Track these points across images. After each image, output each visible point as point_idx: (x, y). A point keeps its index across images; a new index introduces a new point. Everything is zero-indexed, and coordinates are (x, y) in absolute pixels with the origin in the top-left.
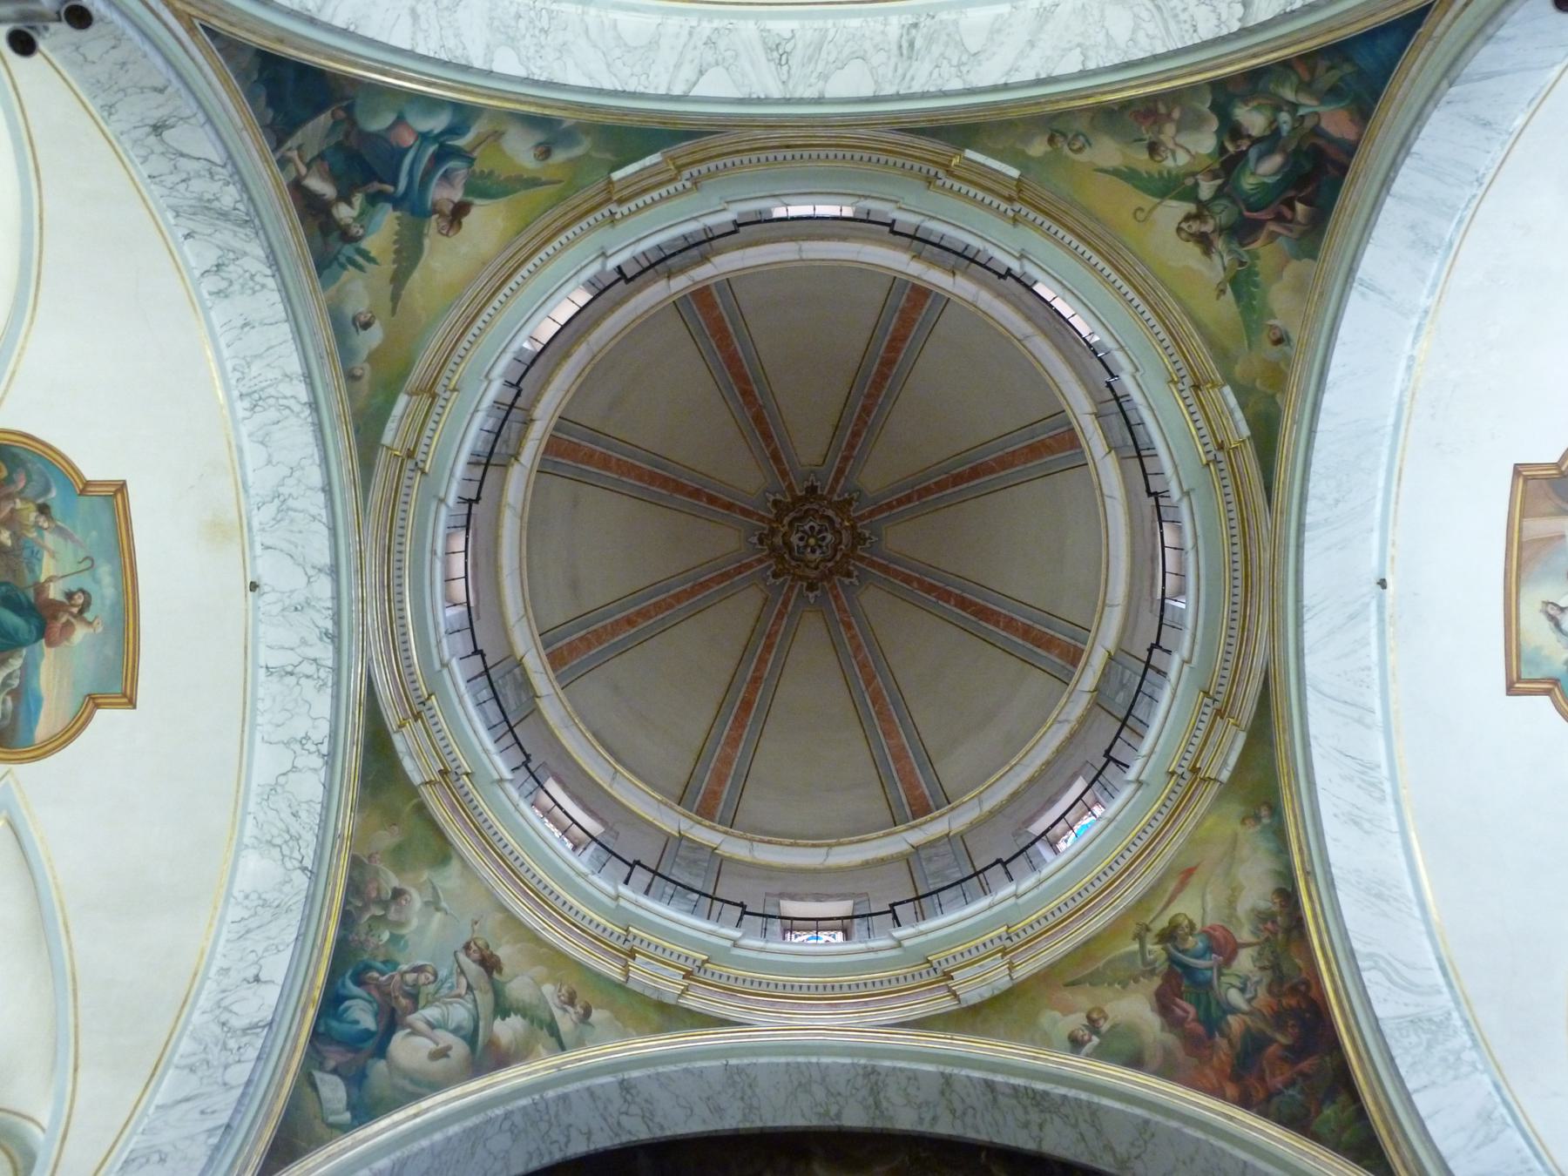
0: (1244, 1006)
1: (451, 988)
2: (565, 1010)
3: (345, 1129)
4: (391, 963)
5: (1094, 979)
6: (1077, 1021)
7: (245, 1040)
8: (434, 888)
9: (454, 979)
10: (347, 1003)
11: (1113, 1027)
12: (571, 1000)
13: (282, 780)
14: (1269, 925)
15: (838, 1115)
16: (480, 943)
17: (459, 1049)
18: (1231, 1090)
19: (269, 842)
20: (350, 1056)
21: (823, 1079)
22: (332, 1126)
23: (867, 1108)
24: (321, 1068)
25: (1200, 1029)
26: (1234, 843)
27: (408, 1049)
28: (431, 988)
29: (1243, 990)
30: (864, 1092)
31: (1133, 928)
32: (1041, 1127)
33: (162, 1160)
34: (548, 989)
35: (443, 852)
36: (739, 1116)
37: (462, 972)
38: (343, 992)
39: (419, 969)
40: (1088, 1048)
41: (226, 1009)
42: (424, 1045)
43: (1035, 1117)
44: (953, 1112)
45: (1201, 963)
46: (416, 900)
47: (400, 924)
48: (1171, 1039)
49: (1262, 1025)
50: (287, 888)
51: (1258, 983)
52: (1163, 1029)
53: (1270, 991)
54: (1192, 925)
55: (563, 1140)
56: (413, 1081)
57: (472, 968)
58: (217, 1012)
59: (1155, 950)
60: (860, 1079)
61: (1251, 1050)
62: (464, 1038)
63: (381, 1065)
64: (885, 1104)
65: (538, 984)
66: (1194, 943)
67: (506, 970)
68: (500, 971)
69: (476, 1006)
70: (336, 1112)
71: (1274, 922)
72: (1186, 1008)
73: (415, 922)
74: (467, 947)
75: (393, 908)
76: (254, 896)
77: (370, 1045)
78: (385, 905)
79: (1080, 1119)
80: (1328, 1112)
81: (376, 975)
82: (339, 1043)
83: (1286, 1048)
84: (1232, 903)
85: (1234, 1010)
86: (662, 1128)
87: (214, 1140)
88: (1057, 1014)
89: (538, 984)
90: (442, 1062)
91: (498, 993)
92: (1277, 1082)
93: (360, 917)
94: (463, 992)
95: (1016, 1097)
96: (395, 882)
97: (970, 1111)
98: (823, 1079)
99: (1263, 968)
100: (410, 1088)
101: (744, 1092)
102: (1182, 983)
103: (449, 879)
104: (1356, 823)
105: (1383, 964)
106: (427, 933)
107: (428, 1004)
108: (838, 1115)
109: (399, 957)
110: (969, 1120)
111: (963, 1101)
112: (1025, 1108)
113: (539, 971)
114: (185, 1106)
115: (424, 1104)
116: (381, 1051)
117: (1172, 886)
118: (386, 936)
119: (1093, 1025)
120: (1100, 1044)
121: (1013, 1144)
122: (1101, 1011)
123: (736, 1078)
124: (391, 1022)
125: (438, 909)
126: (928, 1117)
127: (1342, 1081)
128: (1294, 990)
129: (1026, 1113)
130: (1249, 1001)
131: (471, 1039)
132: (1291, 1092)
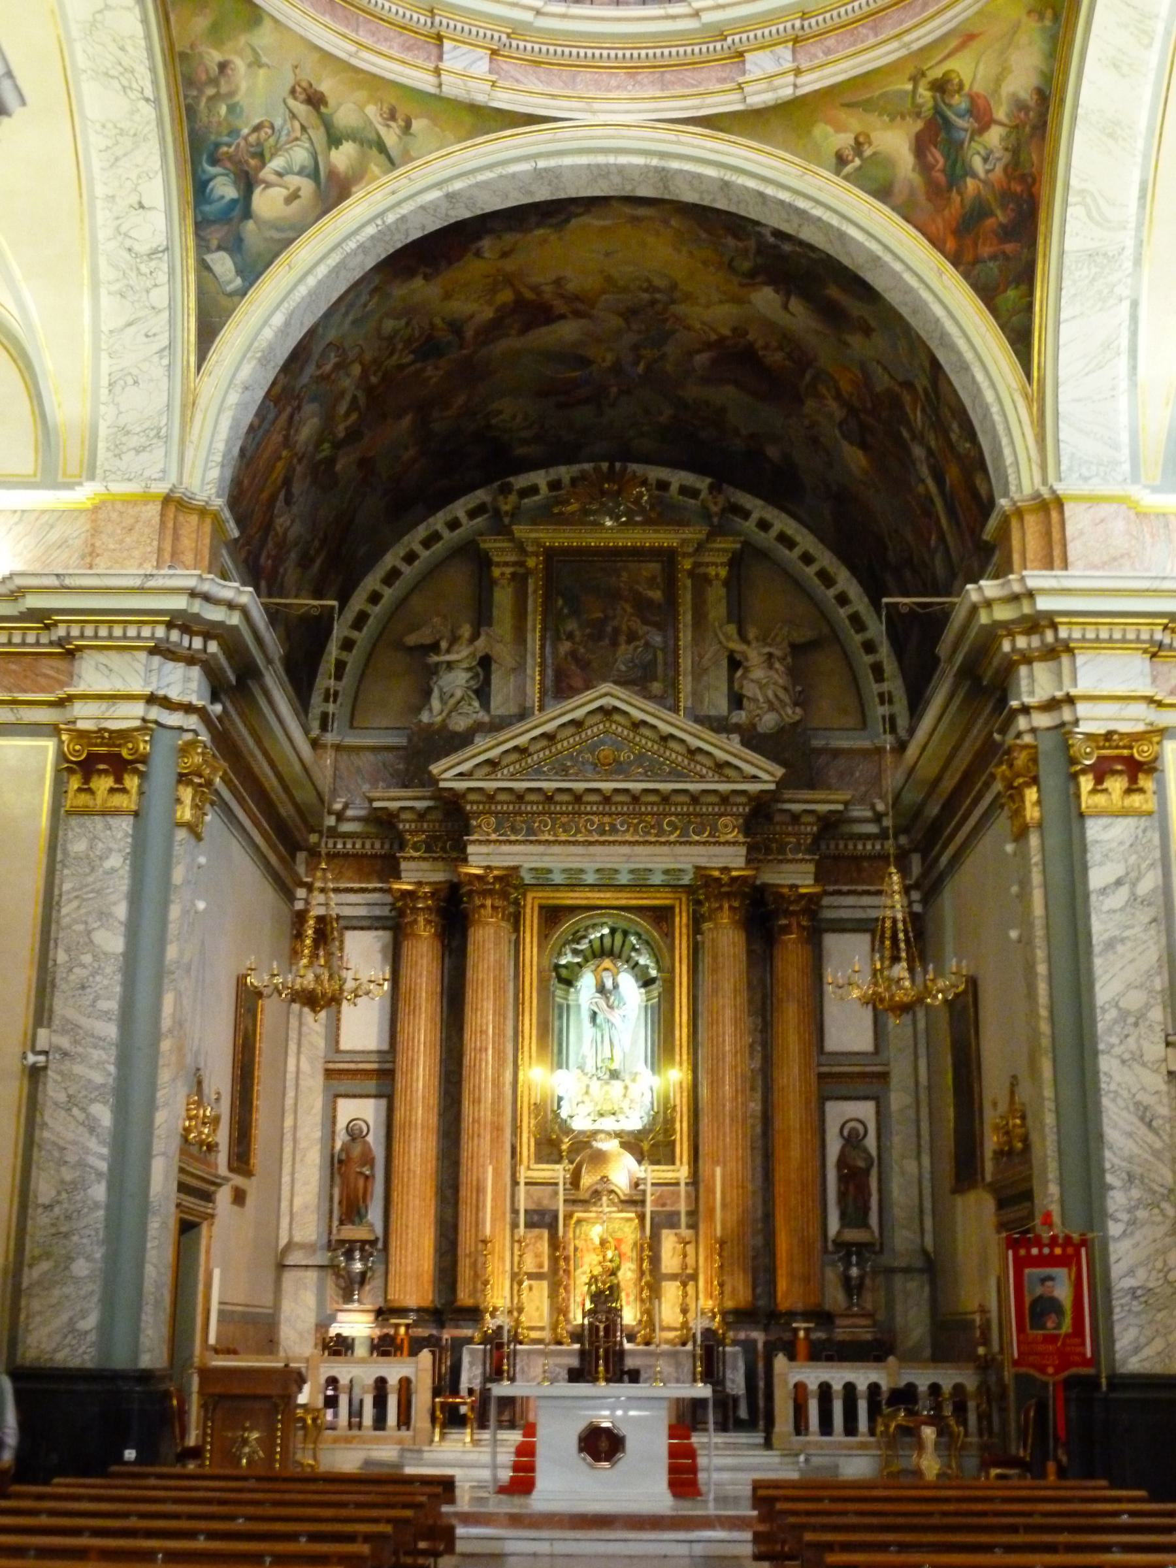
0: (982, 174)
1: (288, 134)
2: (388, 126)
3: (243, 293)
4: (234, 132)
5: (867, 106)
6: (844, 140)
7: (153, 264)
8: (253, 50)
9: (289, 125)
10: (211, 184)
11: (875, 154)
12: (392, 116)
13: (99, 17)
14: (1022, 115)
16: (304, 84)
17: (306, 186)
18: (951, 244)
19: (106, 74)
20: (226, 228)
22: (230, 295)
24: (209, 250)
25: (941, 178)
26: (1016, 28)
27: (268, 202)
28: (272, 141)
29: (985, 160)
31: (910, 70)
33: (136, 382)
37: (294, 116)
38: (205, 177)
39: (257, 128)
40: (849, 169)
41: (126, 235)
42: (277, 194)
45: (960, 123)
46: (240, 64)
47: (232, 94)
48: (916, 179)
49: (990, 197)
50: (137, 117)
51: (999, 159)
52: (914, 170)
53: (1005, 169)
54: (961, 86)
56: (279, 229)
57: (301, 109)
58: (120, 238)
59: (925, 95)
61: (975, 215)
62: (308, 176)
63: (250, 225)
64: (672, 188)
65: (361, 108)
66: (960, 102)
67: (331, 101)
68: (326, 104)
69: (312, 143)
70: (230, 282)
71: (1027, 114)
72: (937, 157)
73: (244, 86)
74: (293, 92)
75: (223, 82)
76: (109, 125)
77: (237, 213)
78: (214, 82)
81: (225, 149)
82: (214, 222)
83: (1001, 225)
84: (998, 81)
85: (974, 175)
87: (165, 362)
88: (830, 129)
89: (361, 108)
90: (296, 204)
91: (327, 125)
92: (985, 251)
93: (198, 104)
94: (298, 134)
96: (215, 56)
99: (1006, 149)
100: (277, 235)
102: (938, 135)
103: (264, 37)
104: (1116, 66)
105: (1088, 200)
106: (257, 93)
107: (273, 155)
108: (633, 190)
109: (238, 123)
113: (361, 95)
114: (133, 329)
116: (247, 214)
117: (953, 43)
118: (223, 110)
119: (858, 147)
120: (860, 168)
122: (868, 136)
124: (248, 183)
125: (260, 65)
127: (1025, 275)
128: (1022, 178)
130: (988, 172)
131: (315, 175)
132: (991, 264)
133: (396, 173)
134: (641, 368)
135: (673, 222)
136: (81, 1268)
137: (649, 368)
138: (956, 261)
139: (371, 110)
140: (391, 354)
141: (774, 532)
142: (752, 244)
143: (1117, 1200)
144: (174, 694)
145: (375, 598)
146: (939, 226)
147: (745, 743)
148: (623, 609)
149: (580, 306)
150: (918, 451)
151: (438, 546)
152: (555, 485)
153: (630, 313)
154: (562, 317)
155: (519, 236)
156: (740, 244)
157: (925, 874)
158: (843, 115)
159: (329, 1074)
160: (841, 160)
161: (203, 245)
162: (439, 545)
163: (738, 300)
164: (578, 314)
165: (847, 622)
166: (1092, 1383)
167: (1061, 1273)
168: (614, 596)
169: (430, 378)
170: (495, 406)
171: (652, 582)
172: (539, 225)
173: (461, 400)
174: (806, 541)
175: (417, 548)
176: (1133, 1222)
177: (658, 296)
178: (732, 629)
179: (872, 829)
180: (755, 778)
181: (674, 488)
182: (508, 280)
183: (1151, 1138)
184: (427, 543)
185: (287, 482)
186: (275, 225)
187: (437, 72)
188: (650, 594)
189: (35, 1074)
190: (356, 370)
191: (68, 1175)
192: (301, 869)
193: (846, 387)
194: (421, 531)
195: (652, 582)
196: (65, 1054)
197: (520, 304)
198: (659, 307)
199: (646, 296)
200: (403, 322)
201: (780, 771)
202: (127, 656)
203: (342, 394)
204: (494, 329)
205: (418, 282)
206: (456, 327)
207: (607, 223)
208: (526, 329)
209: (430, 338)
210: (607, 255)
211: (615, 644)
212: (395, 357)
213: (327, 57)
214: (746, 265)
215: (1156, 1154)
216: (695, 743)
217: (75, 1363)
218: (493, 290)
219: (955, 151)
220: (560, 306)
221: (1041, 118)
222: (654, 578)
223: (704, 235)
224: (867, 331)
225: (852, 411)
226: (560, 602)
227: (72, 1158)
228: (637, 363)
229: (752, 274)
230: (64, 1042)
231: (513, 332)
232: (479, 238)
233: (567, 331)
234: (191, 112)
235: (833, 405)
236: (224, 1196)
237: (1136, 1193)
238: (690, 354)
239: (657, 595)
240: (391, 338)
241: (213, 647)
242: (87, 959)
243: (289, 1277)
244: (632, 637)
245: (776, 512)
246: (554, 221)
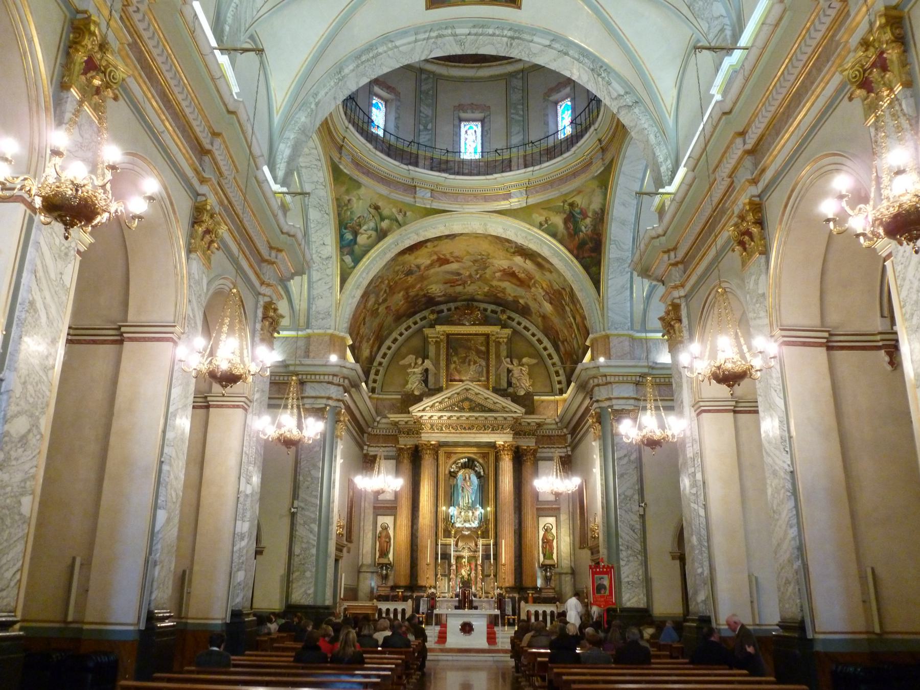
3: (354, 267)
4: (352, 219)
5: (549, 209)
6: (542, 219)
12: (401, 211)
17: (374, 234)
18: (575, 252)
27: (362, 239)
34: (394, 210)
35: (358, 185)
46: (354, 200)
48: (565, 232)
57: (372, 211)
59: (567, 207)
63: (356, 247)
66: (577, 210)
72: (571, 225)
73: (355, 206)
78: (346, 205)
84: (589, 205)
92: (586, 255)
96: (347, 198)
102: (571, 218)
103: (362, 191)
106: (359, 207)
115: (370, 254)
119: (546, 221)
124: (356, 234)
127: (598, 264)
131: (376, 230)
133: (403, 228)
136: (308, 574)
138: (577, 257)
139: (394, 210)
141: (522, 326)
143: (623, 554)
144: (334, 396)
146: (571, 246)
147: (513, 401)
149: (458, 259)
150: (567, 309)
152: (449, 310)
153: (475, 261)
157: (572, 442)
158: (542, 211)
159: (375, 508)
160: (541, 225)
161: (342, 254)
164: (458, 261)
166: (615, 610)
167: (606, 576)
168: (470, 349)
173: (419, 286)
174: (533, 329)
175: (403, 331)
176: (628, 561)
178: (508, 360)
179: (554, 427)
181: (489, 310)
182: (436, 253)
183: (634, 535)
184: (406, 330)
185: (364, 319)
186: (363, 246)
187: (414, 198)
189: (293, 515)
190: (386, 282)
191: (304, 546)
192: (366, 439)
193: (545, 286)
194: (405, 325)
196: (303, 508)
197: (439, 259)
201: (524, 410)
202: (320, 384)
204: (431, 265)
206: (418, 267)
208: (440, 266)
211: (469, 365)
213: (381, 196)
214: (512, 250)
215: (636, 540)
216: (496, 400)
217: (306, 603)
219: (576, 223)
220: (452, 259)
221: (601, 217)
224: (551, 272)
225: (547, 293)
227: (305, 541)
229: (514, 253)
230: (302, 505)
234: (339, 215)
235: (541, 291)
236: (345, 550)
237: (629, 552)
238: (494, 273)
239: (483, 348)
240: (397, 272)
241: (346, 381)
242: (309, 479)
243: (362, 575)
244: (475, 363)
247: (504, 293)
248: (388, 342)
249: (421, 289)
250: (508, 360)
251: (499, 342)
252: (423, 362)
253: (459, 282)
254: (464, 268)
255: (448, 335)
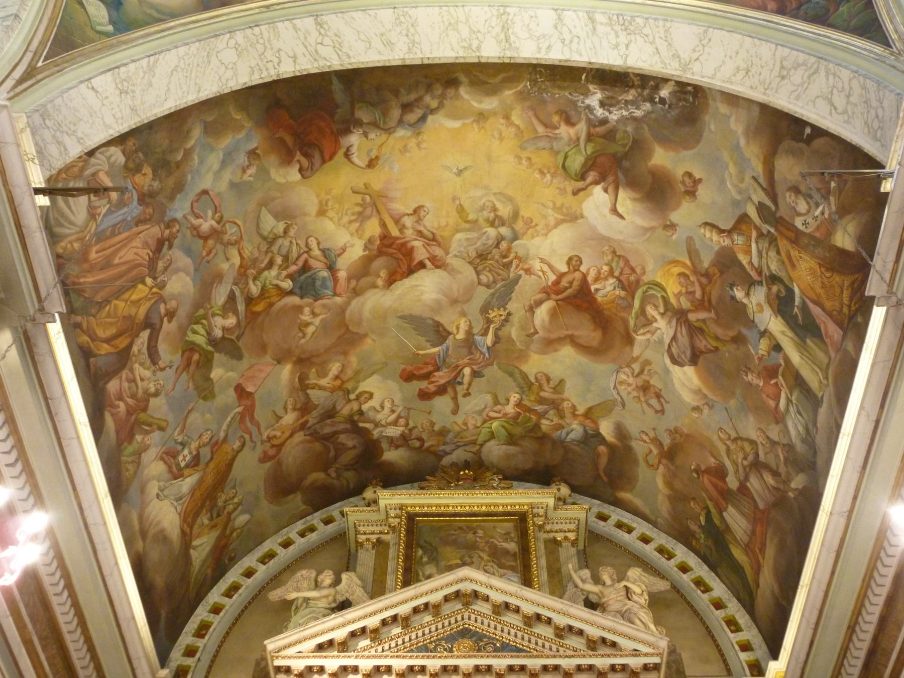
15: (479, 48)
21: (467, 21)
23: (499, 42)
30: (498, 29)
32: (627, 46)
36: (405, 49)
43: (623, 38)
44: (563, 41)
55: (276, 60)
56: (157, 11)
60: (494, 19)
64: (513, 38)
79: (657, 36)
80: (844, 8)
86: (349, 57)
95: (611, 24)
97: (576, 40)
98: (467, 21)
101: (408, 30)
110: (574, 46)
111: (571, 32)
112: (616, 32)
121: (606, 62)
123: (402, 19)
126: (544, 46)
129: (617, 36)
134: (489, 339)
135: (516, 118)
137: (497, 339)
140: (270, 265)
142: (582, 128)
145: (249, 574)
148: (482, 558)
151: (313, 537)
154: (422, 265)
155: (384, 137)
156: (572, 131)
162: (314, 534)
163: (573, 217)
165: (693, 585)
169: (308, 324)
170: (366, 386)
171: (506, 536)
172: (400, 122)
173: (335, 368)
177: (504, 231)
180: (636, 653)
188: (505, 545)
193: (673, 287)
194: (300, 525)
195: (506, 536)
198: (504, 245)
199: (492, 232)
200: (281, 227)
203: (219, 277)
204: (363, 270)
205: (293, 174)
207: (457, 124)
208: (390, 282)
209: (306, 268)
210: (460, 173)
212: (274, 272)
214: (576, 162)
218: (362, 217)
222: (508, 534)
223: (541, 129)
226: (420, 552)
228: (485, 333)
231: (380, 282)
232: (347, 131)
233: (425, 289)
238: (531, 310)
239: (512, 546)
240: (271, 241)
245: (612, 508)
246: (412, 117)
247: (555, 405)
248: (249, 561)
249: (342, 388)
250: (586, 573)
251: (555, 541)
252: (337, 581)
253: (442, 377)
254: (454, 302)
255: (411, 518)
